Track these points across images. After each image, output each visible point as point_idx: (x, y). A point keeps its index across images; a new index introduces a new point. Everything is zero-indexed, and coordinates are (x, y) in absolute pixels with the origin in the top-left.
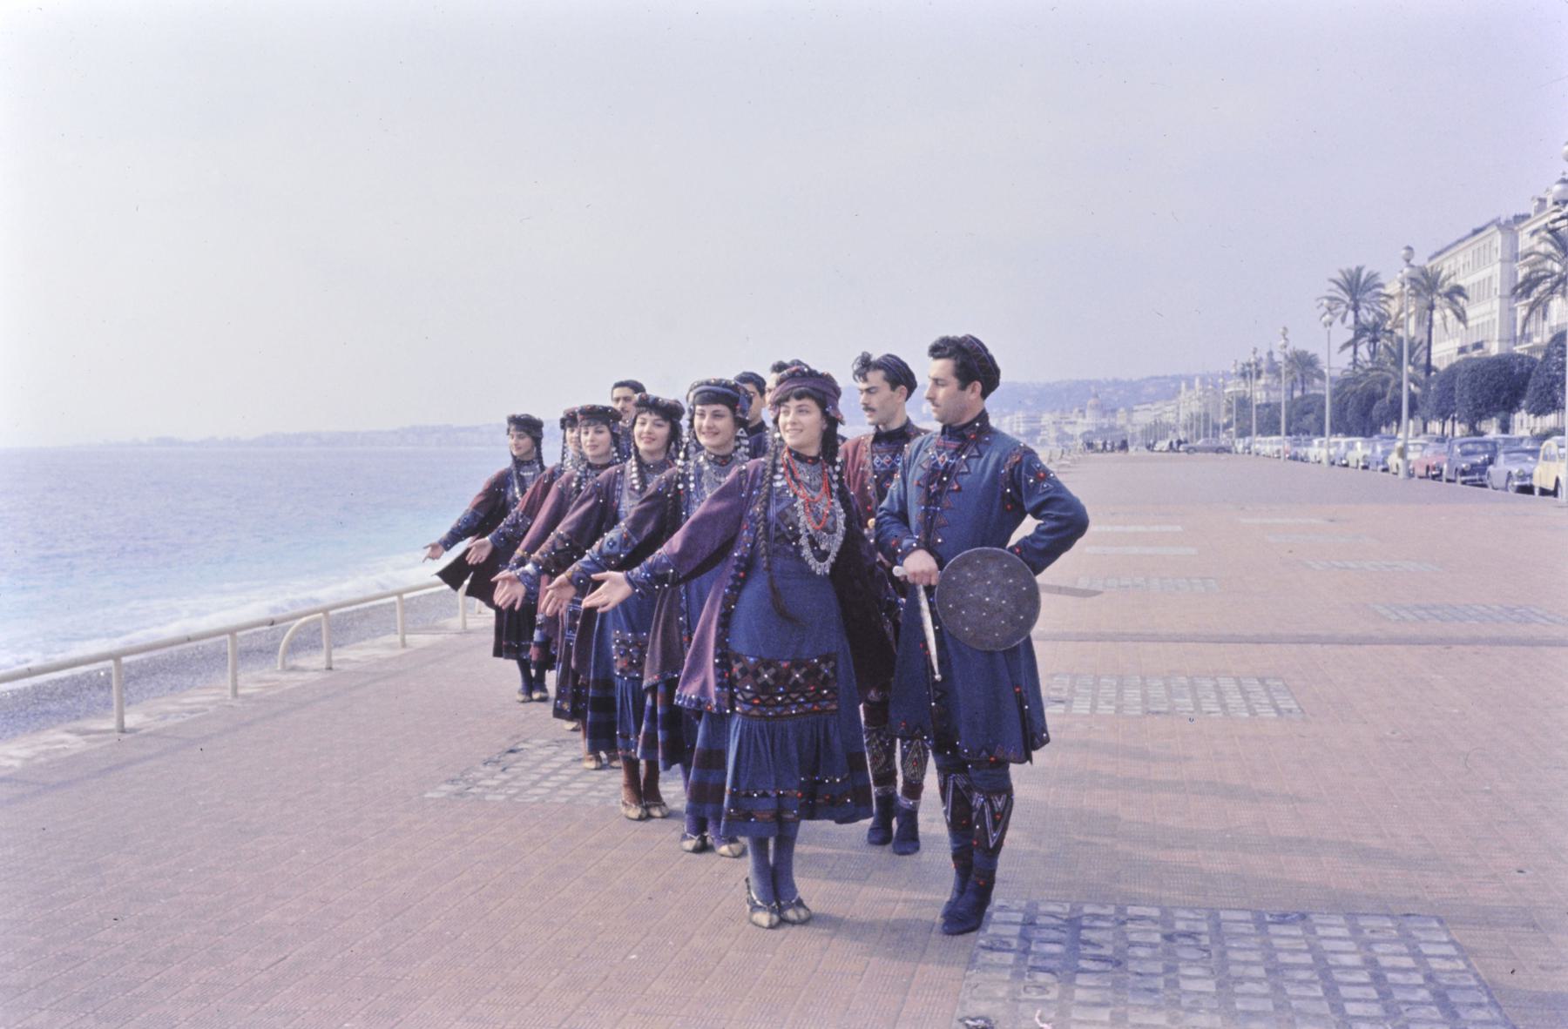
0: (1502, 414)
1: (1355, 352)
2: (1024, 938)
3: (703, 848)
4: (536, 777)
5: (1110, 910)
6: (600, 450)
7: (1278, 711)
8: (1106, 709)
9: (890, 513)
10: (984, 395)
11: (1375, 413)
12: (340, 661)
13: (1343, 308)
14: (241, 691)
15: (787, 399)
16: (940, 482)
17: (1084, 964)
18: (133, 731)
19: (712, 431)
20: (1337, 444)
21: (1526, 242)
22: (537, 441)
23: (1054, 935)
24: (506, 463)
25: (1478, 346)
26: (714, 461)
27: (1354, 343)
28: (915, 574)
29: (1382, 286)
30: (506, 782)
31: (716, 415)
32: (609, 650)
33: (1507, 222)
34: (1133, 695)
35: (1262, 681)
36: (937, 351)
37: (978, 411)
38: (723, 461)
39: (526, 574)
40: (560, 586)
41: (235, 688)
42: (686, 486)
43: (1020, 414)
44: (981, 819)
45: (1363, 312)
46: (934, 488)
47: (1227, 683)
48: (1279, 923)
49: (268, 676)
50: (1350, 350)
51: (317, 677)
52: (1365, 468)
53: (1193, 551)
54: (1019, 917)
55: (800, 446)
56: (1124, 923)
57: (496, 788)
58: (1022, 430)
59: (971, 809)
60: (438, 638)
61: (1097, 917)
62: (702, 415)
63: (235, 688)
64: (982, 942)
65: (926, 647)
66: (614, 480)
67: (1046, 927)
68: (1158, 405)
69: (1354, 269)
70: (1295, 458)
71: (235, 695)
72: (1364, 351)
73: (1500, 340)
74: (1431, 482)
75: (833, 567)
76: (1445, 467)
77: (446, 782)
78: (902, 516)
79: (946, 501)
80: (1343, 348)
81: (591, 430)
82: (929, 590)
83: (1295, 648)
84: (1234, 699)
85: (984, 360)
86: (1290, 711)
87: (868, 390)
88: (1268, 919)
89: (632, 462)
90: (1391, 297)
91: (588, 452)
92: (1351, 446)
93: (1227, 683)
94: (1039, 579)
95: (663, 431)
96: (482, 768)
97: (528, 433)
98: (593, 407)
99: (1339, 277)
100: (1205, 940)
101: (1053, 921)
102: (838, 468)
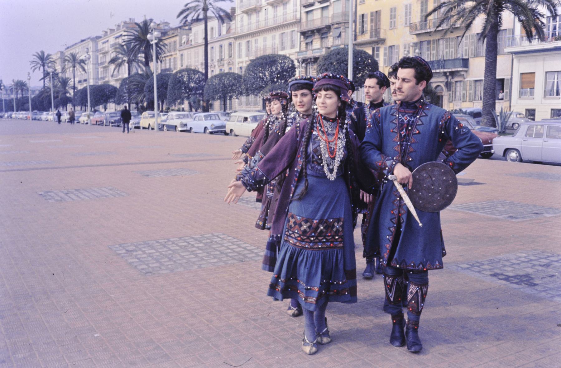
0: (104, 104)
1: (44, 82)
13: (39, 65)
21: (100, 46)
25: (85, 80)
27: (44, 78)
33: (94, 38)
45: (46, 67)
50: (43, 81)
70: (35, 119)
73: (93, 79)
74: (97, 126)
76: (105, 121)
80: (41, 80)
90: (54, 62)
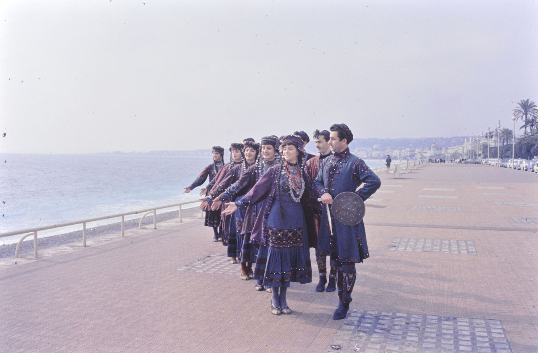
2: (360, 321)
3: (262, 289)
4: (214, 265)
5: (391, 314)
6: (237, 158)
7: (468, 252)
8: (409, 249)
9: (318, 181)
10: (348, 143)
11: (532, 150)
12: (159, 226)
13: (521, 114)
14: (125, 235)
15: (285, 145)
16: (333, 171)
17: (376, 330)
18: (89, 246)
19: (267, 154)
20: (517, 161)
22: (222, 155)
23: (369, 321)
24: (212, 162)
26: (268, 163)
27: (525, 126)
28: (325, 201)
29: (535, 106)
30: (204, 266)
31: (268, 148)
32: (235, 225)
34: (420, 245)
35: (466, 242)
36: (332, 129)
37: (345, 148)
38: (270, 163)
39: (209, 198)
40: (217, 201)
41: (123, 234)
42: (258, 171)
43: (408, 149)
44: (345, 281)
45: (529, 115)
46: (331, 173)
47: (453, 242)
48: (446, 320)
49: (135, 231)
50: (524, 128)
51: (151, 231)
52: (526, 170)
53: (456, 197)
54: (360, 315)
55: (290, 160)
56: (394, 318)
57: (200, 268)
58: (408, 155)
59: (343, 278)
60: (193, 220)
61: (385, 316)
62: (264, 148)
63: (123, 234)
64: (345, 322)
65: (329, 225)
66: (238, 169)
67: (368, 318)
68: (456, 147)
69: (526, 100)
70: (502, 166)
71: (123, 236)
72: (528, 129)
75: (301, 200)
77: (185, 266)
78: (322, 182)
79: (335, 177)
80: (521, 128)
81: (235, 151)
82: (330, 205)
83: (480, 231)
84: (454, 248)
85: (347, 132)
86: (472, 252)
87: (319, 142)
88: (443, 319)
89: (244, 163)
91: (233, 158)
92: (521, 163)
93: (453, 242)
94: (365, 202)
95: (254, 153)
96: (198, 262)
97: (219, 153)
98: (235, 144)
99: (520, 102)
100: (419, 325)
101: (371, 316)
102: (302, 167)
